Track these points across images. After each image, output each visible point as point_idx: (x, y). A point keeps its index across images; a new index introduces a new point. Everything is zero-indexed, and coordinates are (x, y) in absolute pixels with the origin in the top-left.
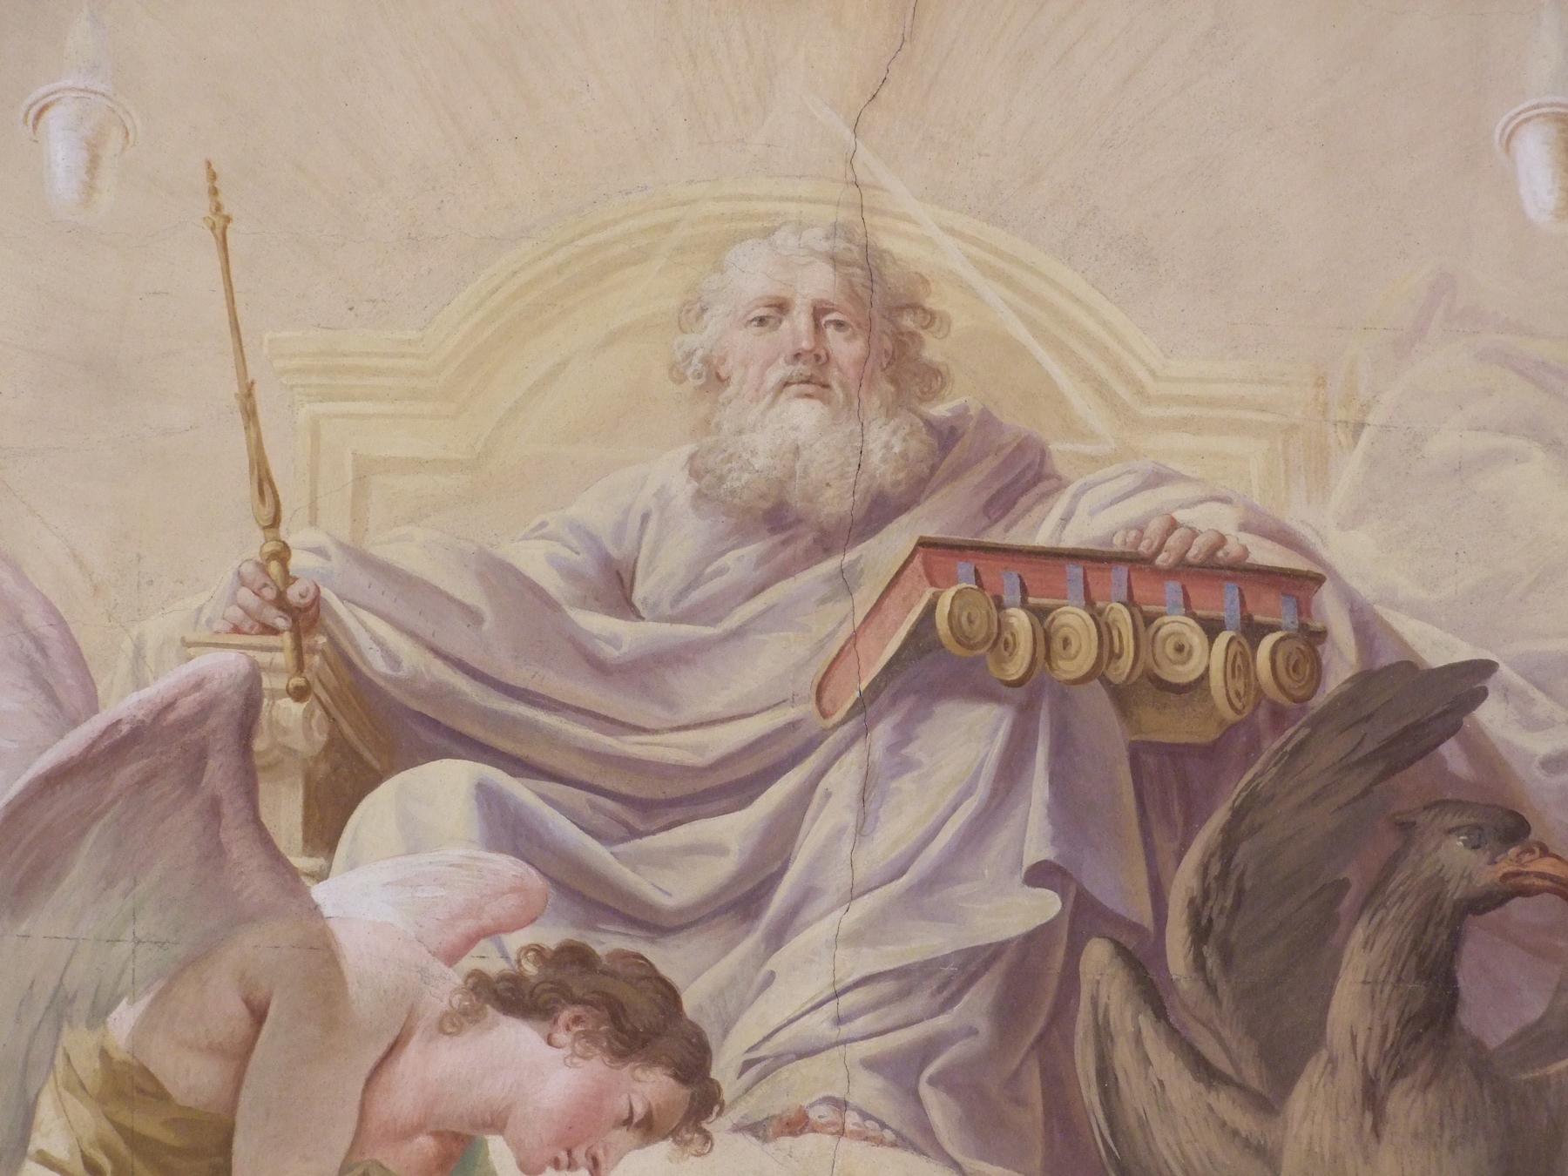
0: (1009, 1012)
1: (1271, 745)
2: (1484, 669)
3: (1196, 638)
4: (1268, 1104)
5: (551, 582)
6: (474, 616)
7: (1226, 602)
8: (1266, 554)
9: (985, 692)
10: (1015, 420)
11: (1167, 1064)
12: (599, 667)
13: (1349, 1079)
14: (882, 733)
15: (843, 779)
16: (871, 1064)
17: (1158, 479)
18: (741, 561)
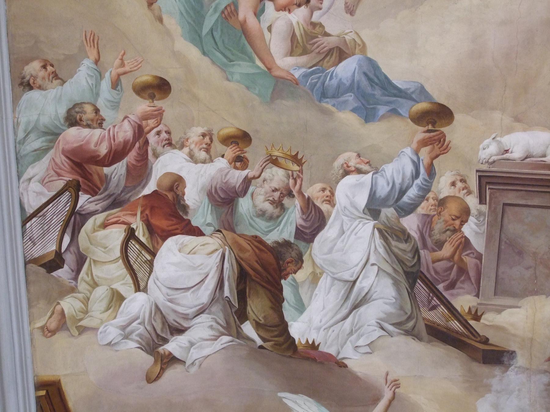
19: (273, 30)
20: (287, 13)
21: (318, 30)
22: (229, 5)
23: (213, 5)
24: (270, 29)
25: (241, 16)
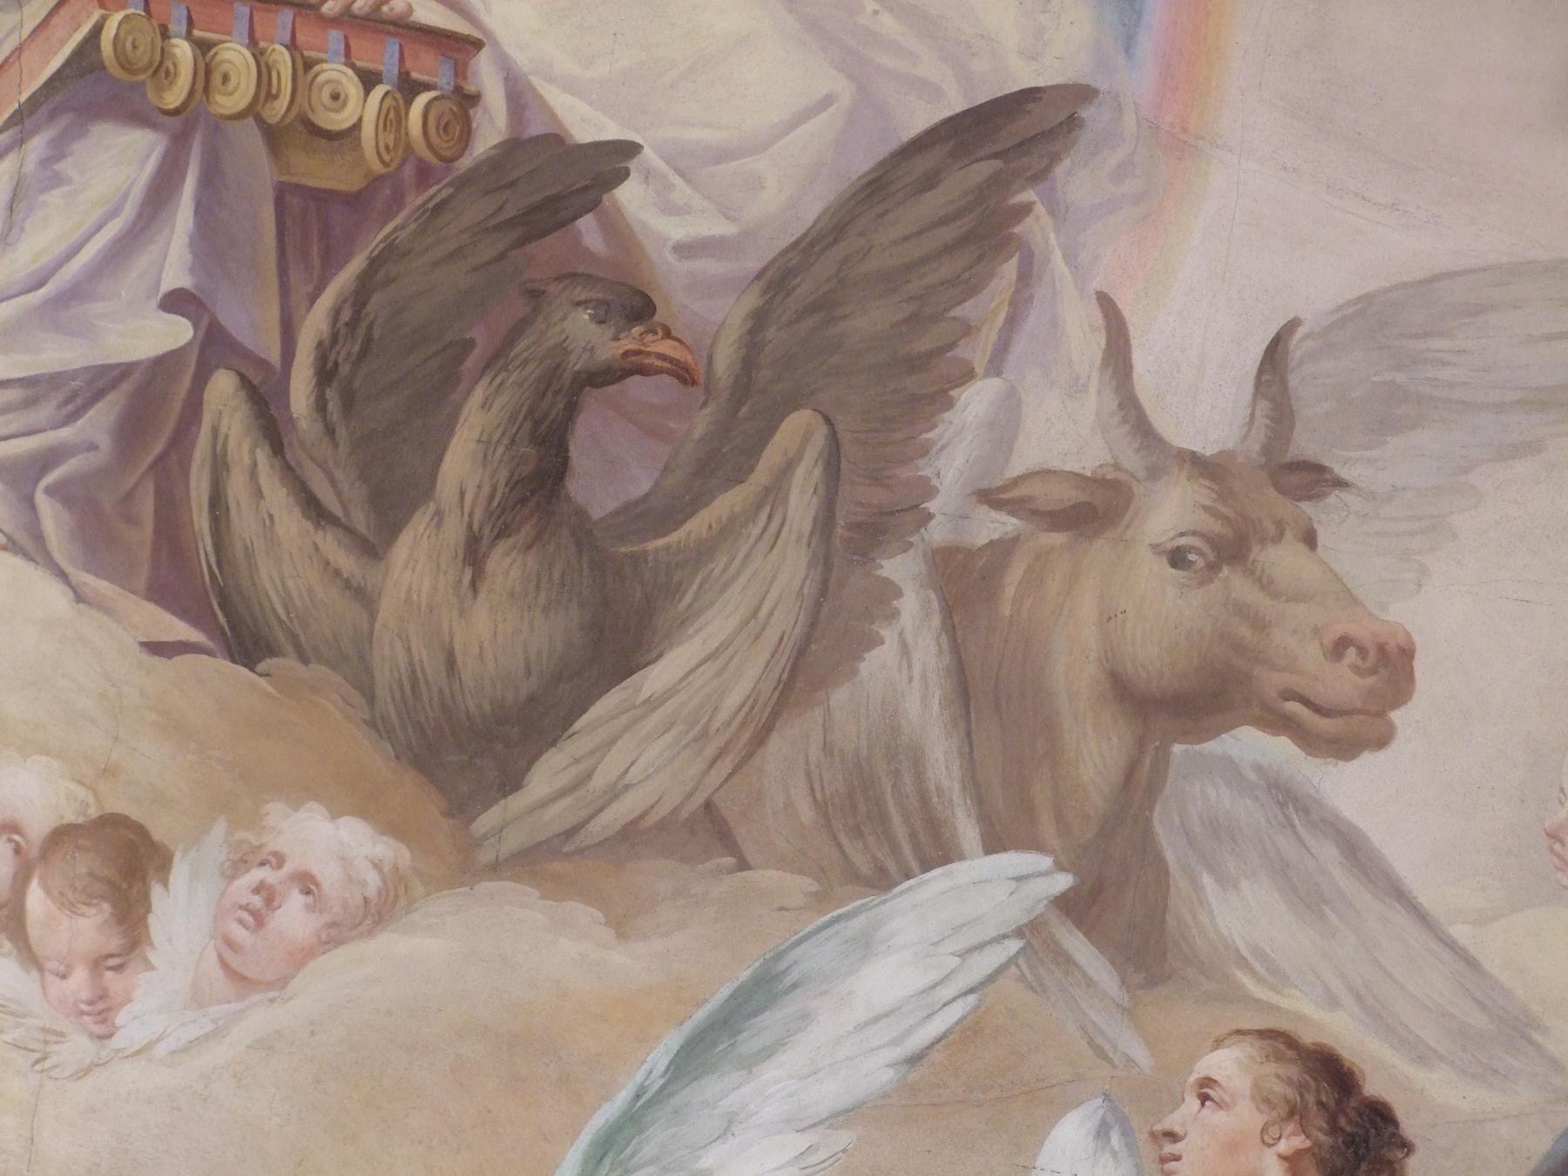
0: (131, 431)
1: (414, 201)
2: (629, 150)
3: (352, 87)
4: (373, 549)
7: (386, 56)
9: (140, 118)
11: (278, 497)
13: (454, 533)
14: (37, 145)
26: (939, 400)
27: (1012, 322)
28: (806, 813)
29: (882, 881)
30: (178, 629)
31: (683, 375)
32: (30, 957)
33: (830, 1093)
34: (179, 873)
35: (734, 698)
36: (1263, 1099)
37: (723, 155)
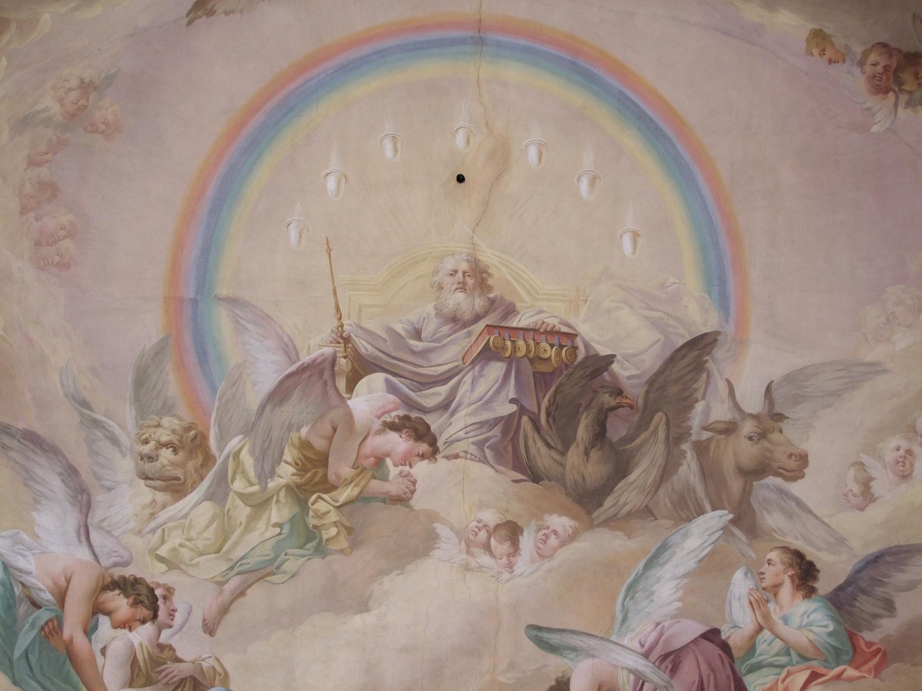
0: (505, 432)
1: (565, 372)
2: (614, 356)
3: (548, 348)
4: (563, 454)
5: (403, 333)
6: (385, 341)
7: (555, 340)
8: (564, 329)
9: (500, 359)
10: (508, 298)
11: (540, 444)
12: (413, 353)
13: (582, 448)
14: (477, 368)
15: (468, 379)
16: (473, 443)
17: (540, 312)
18: (446, 329)
19: (108, 653)
20: (126, 631)
21: (166, 653)
22: (51, 620)
23: (30, 619)
24: (103, 651)
25: (66, 634)
26: (691, 407)
27: (706, 387)
28: (669, 506)
29: (689, 520)
30: (520, 476)
31: (631, 407)
32: (492, 555)
33: (681, 571)
34: (525, 533)
35: (650, 481)
36: (783, 563)
37: (635, 355)
